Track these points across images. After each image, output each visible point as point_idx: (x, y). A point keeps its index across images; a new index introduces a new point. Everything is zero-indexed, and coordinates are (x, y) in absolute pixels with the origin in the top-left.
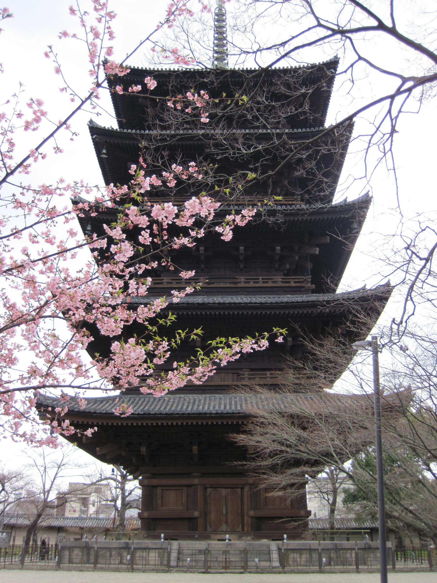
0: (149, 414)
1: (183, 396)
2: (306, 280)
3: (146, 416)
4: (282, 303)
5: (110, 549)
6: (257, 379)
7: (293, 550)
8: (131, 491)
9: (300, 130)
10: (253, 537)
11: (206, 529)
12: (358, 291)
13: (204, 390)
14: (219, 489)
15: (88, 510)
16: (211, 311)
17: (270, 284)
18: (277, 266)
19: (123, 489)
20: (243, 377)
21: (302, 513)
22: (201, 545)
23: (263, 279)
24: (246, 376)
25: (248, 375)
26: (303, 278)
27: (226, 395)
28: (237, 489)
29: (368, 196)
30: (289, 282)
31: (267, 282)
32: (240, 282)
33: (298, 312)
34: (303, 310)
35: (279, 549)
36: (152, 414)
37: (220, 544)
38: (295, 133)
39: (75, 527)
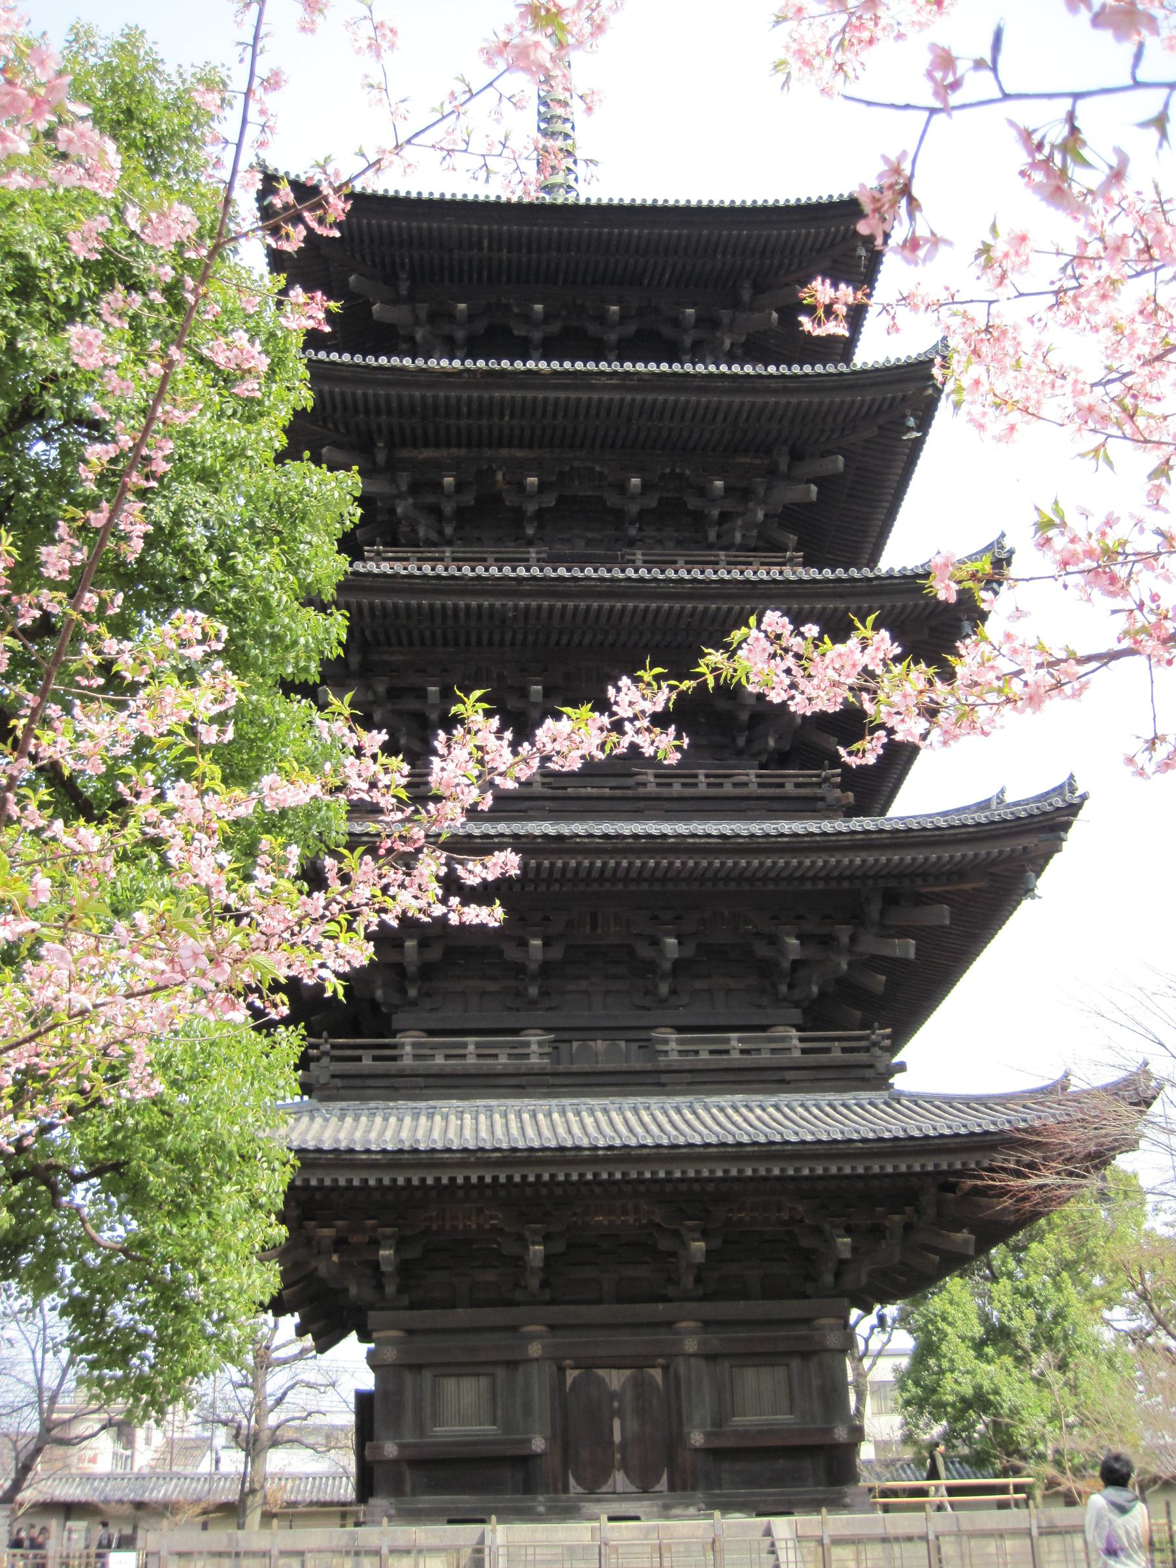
0: (415, 1151)
1: (493, 1102)
2: (826, 780)
3: (406, 1156)
4: (782, 835)
5: (300, 1554)
6: (704, 1056)
7: (838, 1541)
8: (285, 1394)
9: (807, 369)
10: (702, 1506)
11: (566, 1489)
12: (984, 805)
13: (553, 1086)
14: (601, 1372)
15: (132, 1456)
16: (580, 858)
17: (728, 789)
18: (741, 742)
19: (256, 1386)
20: (665, 1048)
21: (841, 1434)
22: (576, 1532)
23: (707, 776)
24: (673, 1045)
25: (680, 1042)
26: (818, 776)
27: (617, 1100)
28: (652, 1371)
29: (1002, 548)
30: (782, 785)
31: (721, 785)
32: (644, 785)
33: (826, 862)
34: (839, 856)
35: (799, 1538)
36: (425, 1152)
37: (627, 1527)
38: (795, 377)
39: (121, 1502)
